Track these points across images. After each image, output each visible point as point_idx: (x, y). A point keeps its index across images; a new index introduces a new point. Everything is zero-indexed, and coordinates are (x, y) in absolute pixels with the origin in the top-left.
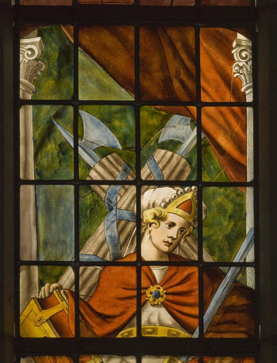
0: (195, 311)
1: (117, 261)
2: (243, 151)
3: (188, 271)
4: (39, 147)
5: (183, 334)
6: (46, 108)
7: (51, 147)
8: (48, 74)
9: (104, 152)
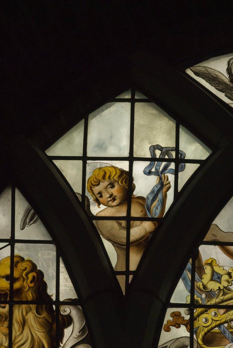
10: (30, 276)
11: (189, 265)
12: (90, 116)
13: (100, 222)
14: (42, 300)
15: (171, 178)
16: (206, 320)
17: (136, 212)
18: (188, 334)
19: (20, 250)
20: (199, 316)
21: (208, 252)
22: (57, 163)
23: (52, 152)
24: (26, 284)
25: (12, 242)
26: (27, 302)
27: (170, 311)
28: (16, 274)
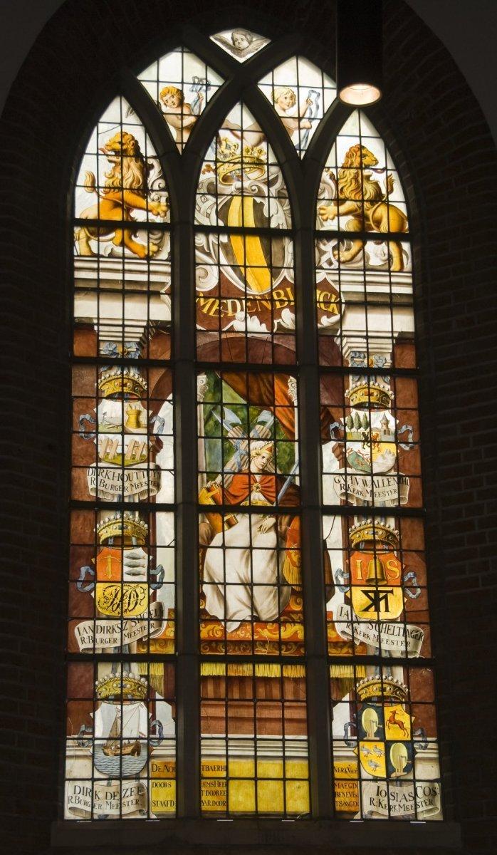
0: (274, 495)
1: (240, 472)
2: (293, 425)
3: (270, 477)
4: (206, 422)
5: (269, 505)
6: (209, 406)
7: (211, 422)
8: (209, 391)
9: (234, 425)
10: (132, 142)
11: (214, 140)
12: (161, 59)
13: (167, 116)
14: (138, 155)
15: (204, 94)
16: (223, 170)
17: (186, 111)
18: (215, 176)
19: (125, 128)
20: (220, 167)
21: (223, 133)
22: (143, 83)
23: (140, 77)
24: (130, 147)
25: (121, 124)
26: (130, 156)
27: (205, 164)
28: (124, 142)
